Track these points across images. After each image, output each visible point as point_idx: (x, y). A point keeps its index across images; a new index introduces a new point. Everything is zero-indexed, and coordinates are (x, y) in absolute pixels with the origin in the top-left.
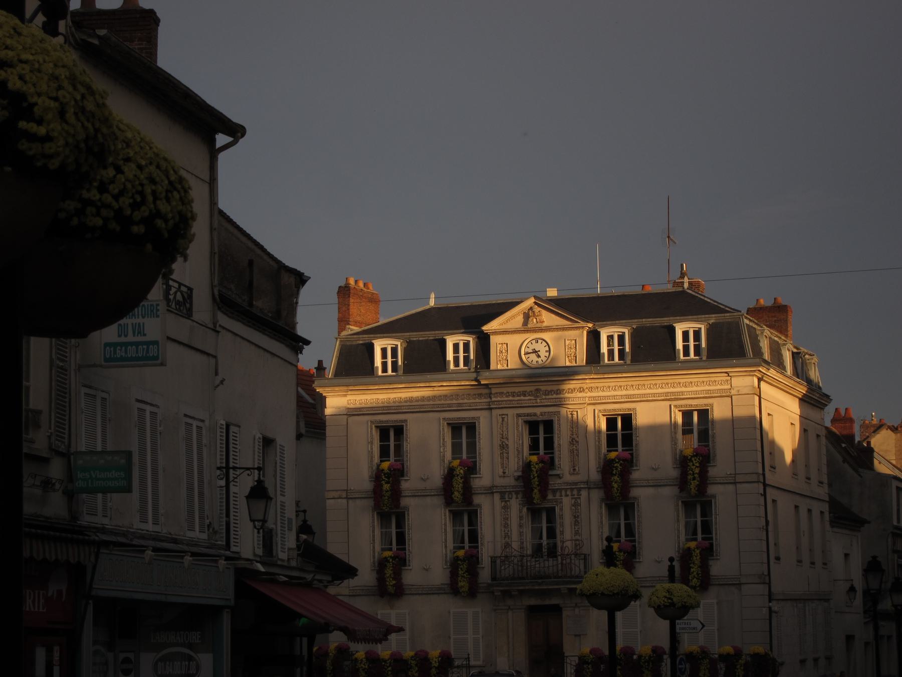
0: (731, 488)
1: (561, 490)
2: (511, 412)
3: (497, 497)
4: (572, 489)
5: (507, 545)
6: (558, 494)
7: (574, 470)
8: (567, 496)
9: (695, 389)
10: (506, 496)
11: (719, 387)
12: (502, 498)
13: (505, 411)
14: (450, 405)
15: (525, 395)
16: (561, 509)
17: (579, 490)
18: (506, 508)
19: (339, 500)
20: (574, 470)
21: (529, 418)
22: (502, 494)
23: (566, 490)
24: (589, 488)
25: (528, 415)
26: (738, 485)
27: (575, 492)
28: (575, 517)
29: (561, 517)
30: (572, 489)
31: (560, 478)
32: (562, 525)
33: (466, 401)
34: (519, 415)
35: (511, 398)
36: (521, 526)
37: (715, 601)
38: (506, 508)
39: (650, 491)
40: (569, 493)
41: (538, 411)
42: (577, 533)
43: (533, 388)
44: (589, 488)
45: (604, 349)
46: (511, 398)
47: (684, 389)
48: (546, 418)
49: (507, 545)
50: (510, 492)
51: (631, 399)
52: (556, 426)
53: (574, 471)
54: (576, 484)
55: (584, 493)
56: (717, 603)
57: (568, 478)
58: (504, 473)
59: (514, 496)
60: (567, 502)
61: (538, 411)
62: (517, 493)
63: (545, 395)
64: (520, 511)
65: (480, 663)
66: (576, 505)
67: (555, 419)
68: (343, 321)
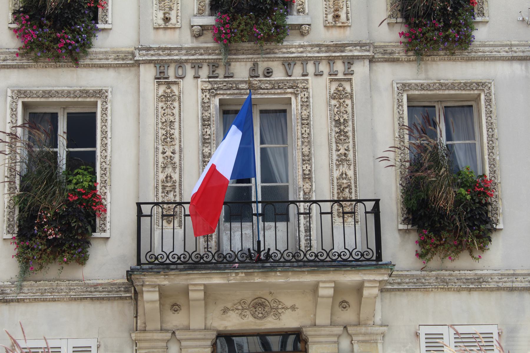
1: (304, 61)
3: (148, 73)
4: (331, 61)
5: (169, 184)
6: (297, 71)
7: (337, 17)
8: (319, 74)
10: (171, 72)
12: (161, 78)
16: (306, 104)
17: (349, 61)
20: (337, 17)
22: (161, 66)
23: (317, 61)
27: (339, 67)
28: (338, 123)
29: (306, 121)
30: (331, 61)
31: (303, 34)
32: (307, 140)
39: (518, 68)
40: (324, 67)
42: (343, 159)
44: (372, 60)
49: (169, 184)
50: (180, 64)
54: (341, 47)
55: (360, 69)
57: (321, 34)
58: (167, 20)
59: (190, 73)
60: (319, 88)
62: (197, 65)
64: (205, 106)
66: (339, 95)
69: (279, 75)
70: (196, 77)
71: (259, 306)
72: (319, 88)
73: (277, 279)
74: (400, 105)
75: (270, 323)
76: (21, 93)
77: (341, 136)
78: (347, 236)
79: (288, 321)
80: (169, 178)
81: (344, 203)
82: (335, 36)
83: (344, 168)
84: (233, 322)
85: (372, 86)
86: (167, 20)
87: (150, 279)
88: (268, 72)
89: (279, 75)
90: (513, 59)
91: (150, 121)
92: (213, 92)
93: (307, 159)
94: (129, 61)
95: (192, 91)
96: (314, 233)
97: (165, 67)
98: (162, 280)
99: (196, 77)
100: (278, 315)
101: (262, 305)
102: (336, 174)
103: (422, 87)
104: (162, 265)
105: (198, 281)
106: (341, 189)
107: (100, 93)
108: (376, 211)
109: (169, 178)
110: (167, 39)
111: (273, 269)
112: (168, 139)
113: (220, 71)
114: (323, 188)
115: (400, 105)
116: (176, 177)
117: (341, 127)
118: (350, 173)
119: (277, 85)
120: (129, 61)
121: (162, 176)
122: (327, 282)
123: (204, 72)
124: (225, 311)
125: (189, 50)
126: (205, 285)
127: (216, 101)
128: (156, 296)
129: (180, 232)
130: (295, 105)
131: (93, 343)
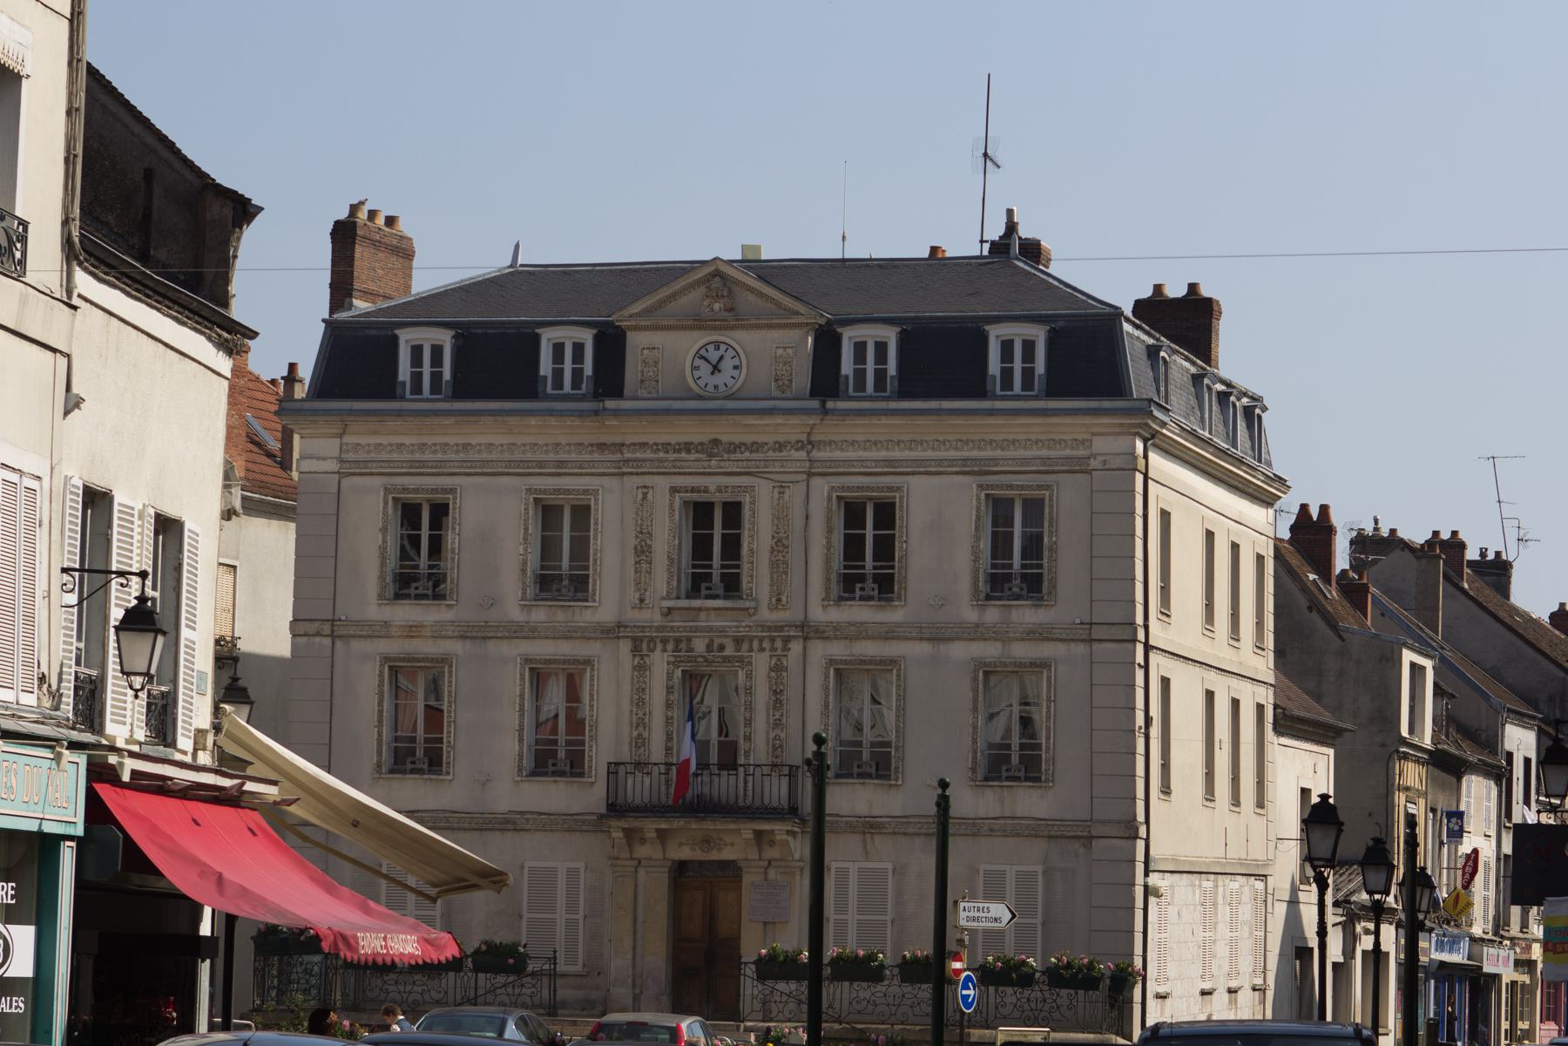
0: (1080, 649)
1: (751, 640)
2: (663, 483)
3: (625, 647)
4: (773, 639)
5: (640, 742)
6: (745, 646)
7: (779, 600)
8: (762, 650)
9: (1021, 453)
10: (644, 646)
11: (1068, 452)
12: (636, 650)
13: (647, 480)
14: (541, 464)
15: (689, 451)
16: (749, 676)
17: (787, 640)
18: (641, 668)
19: (317, 639)
20: (779, 600)
21: (696, 497)
23: (761, 640)
24: (806, 639)
25: (693, 490)
26: (1096, 646)
27: (779, 644)
33: (574, 456)
34: (674, 490)
35: (661, 455)
36: (669, 706)
37: (1039, 869)
38: (641, 668)
39: (924, 648)
40: (766, 645)
41: (712, 482)
42: (778, 724)
43: (705, 438)
45: (847, 366)
46: (661, 455)
47: (999, 453)
48: (728, 497)
49: (640, 742)
50: (651, 640)
51: (894, 467)
52: (746, 513)
53: (777, 603)
55: (796, 647)
56: (1044, 873)
58: (642, 600)
59: (659, 647)
60: (762, 662)
61: (712, 482)
62: (665, 641)
63: (729, 452)
64: (670, 676)
65: (578, 968)
66: (778, 668)
67: (746, 500)
68: (341, 289)
69: (729, 651)
70: (664, 650)
71: (707, 842)
72: (762, 662)
73: (708, 825)
74: (827, 677)
75: (715, 856)
76: (527, 660)
78: (776, 790)
79: (727, 854)
80: (640, 736)
83: (778, 732)
84: (686, 854)
86: (642, 600)
87: (614, 823)
88: (722, 648)
89: (729, 651)
90: (921, 639)
91: (627, 687)
92: (675, 664)
95: (659, 662)
96: (750, 785)
99: (664, 650)
100: (720, 850)
101: (708, 841)
102: (772, 735)
103: (845, 662)
105: (650, 826)
106: (775, 748)
109: (640, 736)
111: (704, 819)
113: (683, 646)
115: (827, 677)
116: (646, 734)
117: (777, 696)
118: (783, 735)
119: (726, 659)
121: (635, 734)
122: (747, 829)
123: (670, 646)
124: (681, 844)
125: (658, 629)
126: (657, 830)
127: (678, 673)
128: (621, 835)
129: (647, 780)
130: (741, 675)
131: (581, 865)
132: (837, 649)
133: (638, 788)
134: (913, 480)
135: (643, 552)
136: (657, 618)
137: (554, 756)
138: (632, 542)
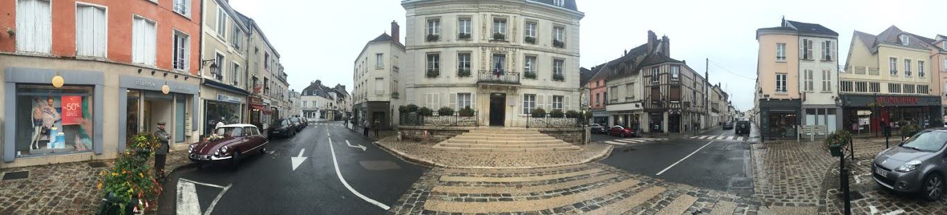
5: (484, 68)
32: (508, 61)
36: (490, 64)
39: (543, 53)
49: (484, 68)
60: (511, 53)
66: (514, 54)
72: (511, 53)
77: (514, 62)
78: (514, 79)
81: (513, 73)
82: (514, 44)
84: (494, 91)
85: (519, 53)
93: (508, 65)
94: (476, 46)
97: (483, 47)
98: (483, 84)
104: (482, 81)
107: (471, 51)
108: (519, 75)
110: (484, 42)
112: (484, 60)
114: (510, 70)
119: (504, 52)
120: (476, 46)
132: (526, 52)
133: (484, 77)
134: (540, 20)
135: (484, 27)
136: (488, 42)
137: (463, 72)
138: (482, 26)
